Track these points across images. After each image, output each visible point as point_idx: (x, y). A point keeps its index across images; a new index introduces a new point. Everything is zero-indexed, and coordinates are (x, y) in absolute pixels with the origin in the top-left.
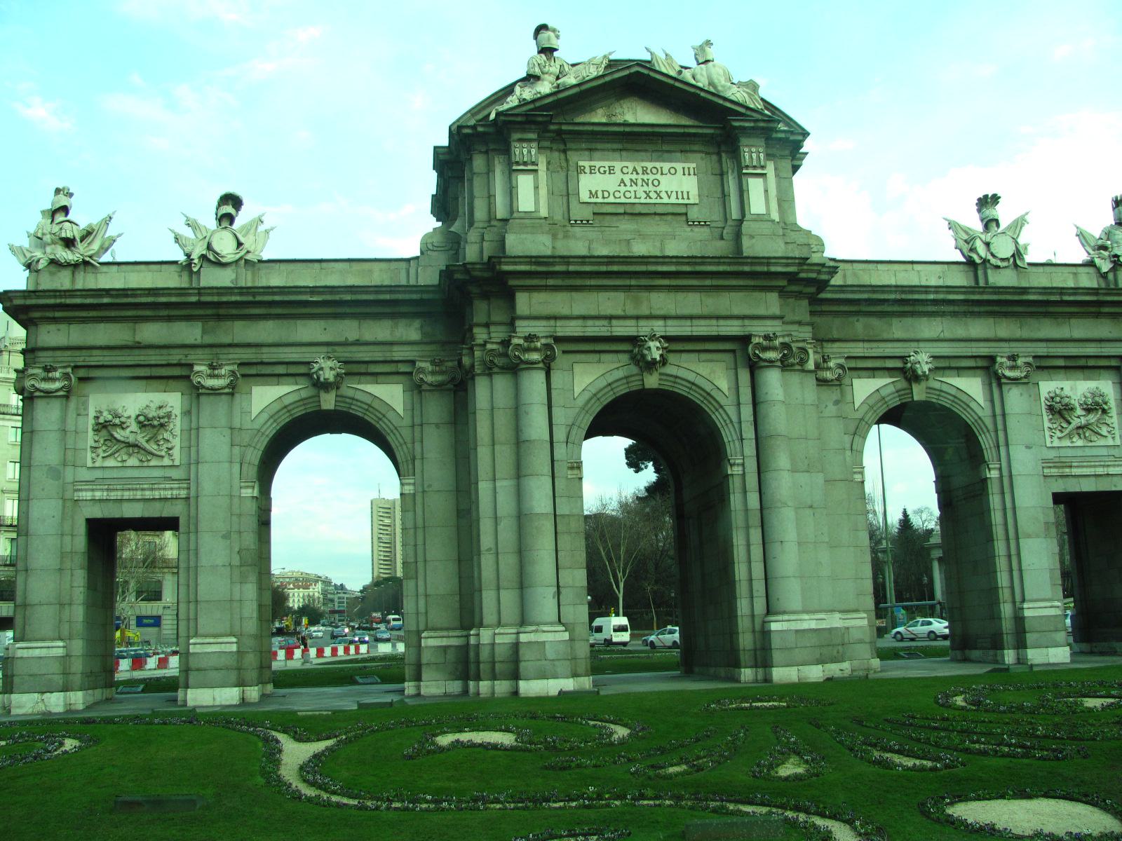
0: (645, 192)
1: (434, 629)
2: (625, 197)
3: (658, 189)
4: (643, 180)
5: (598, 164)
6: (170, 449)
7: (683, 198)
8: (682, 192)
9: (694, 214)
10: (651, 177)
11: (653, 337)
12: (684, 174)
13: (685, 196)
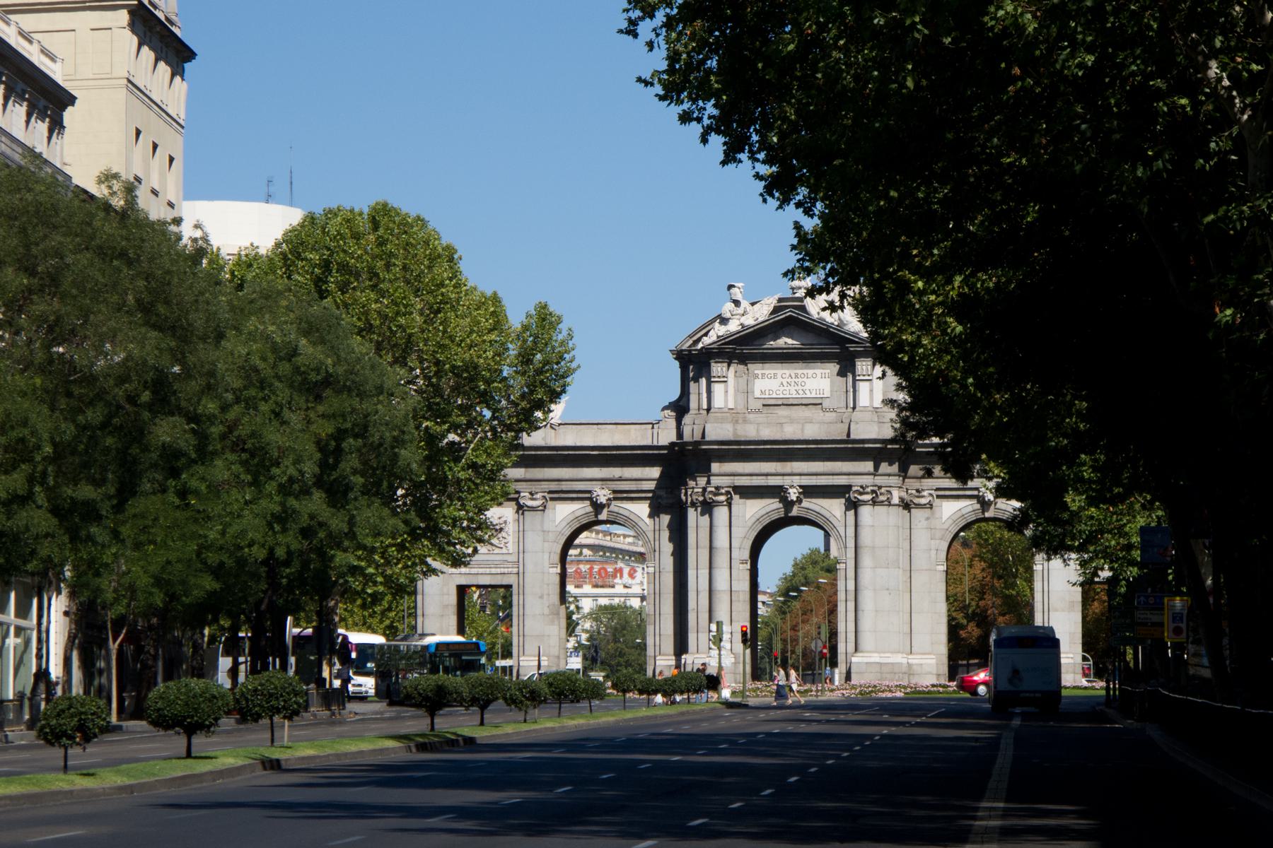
1: (663, 655)
3: (804, 388)
5: (767, 372)
6: (506, 543)
9: (826, 404)
10: (800, 380)
11: (792, 486)
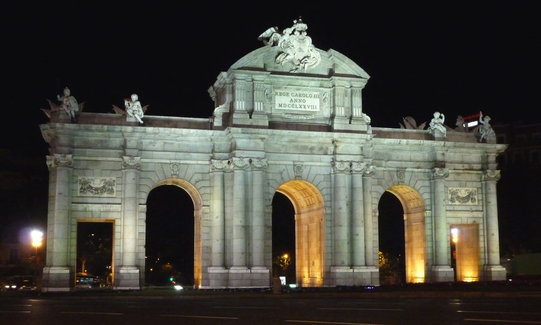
0: (300, 105)
2: (292, 107)
3: (305, 104)
4: (299, 100)
7: (314, 108)
8: (314, 106)
10: (303, 98)
12: (315, 97)
13: (315, 107)
